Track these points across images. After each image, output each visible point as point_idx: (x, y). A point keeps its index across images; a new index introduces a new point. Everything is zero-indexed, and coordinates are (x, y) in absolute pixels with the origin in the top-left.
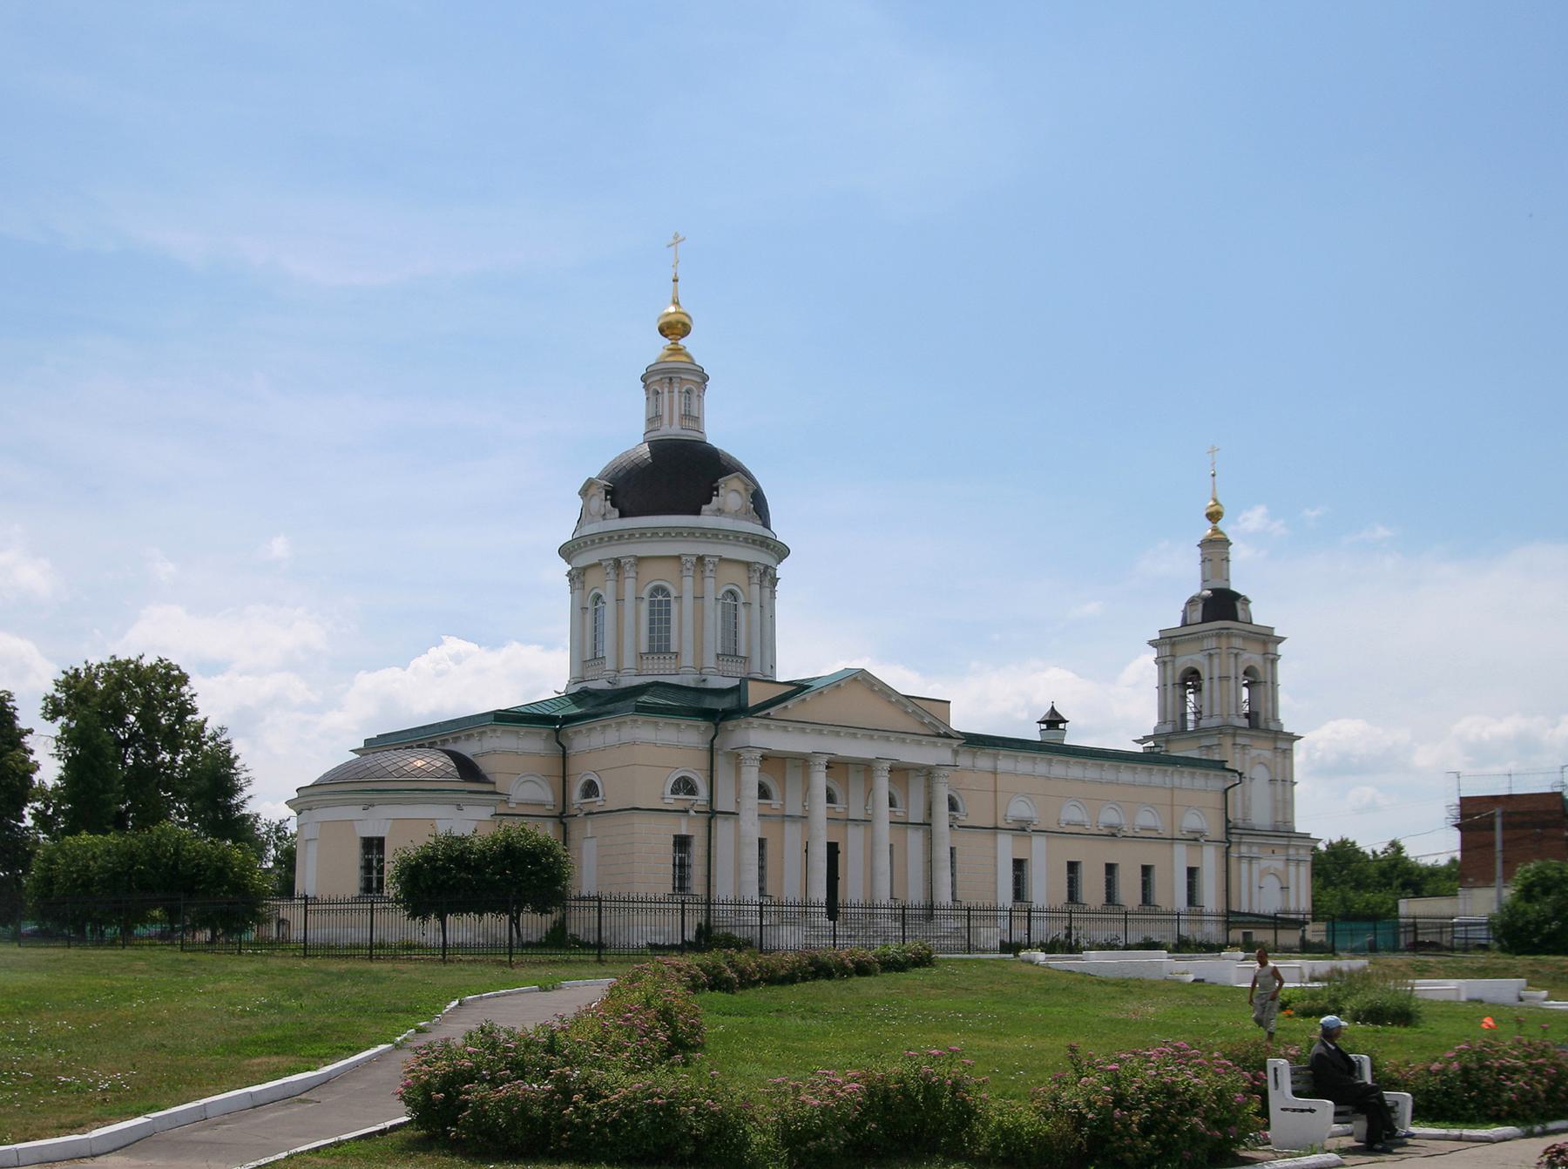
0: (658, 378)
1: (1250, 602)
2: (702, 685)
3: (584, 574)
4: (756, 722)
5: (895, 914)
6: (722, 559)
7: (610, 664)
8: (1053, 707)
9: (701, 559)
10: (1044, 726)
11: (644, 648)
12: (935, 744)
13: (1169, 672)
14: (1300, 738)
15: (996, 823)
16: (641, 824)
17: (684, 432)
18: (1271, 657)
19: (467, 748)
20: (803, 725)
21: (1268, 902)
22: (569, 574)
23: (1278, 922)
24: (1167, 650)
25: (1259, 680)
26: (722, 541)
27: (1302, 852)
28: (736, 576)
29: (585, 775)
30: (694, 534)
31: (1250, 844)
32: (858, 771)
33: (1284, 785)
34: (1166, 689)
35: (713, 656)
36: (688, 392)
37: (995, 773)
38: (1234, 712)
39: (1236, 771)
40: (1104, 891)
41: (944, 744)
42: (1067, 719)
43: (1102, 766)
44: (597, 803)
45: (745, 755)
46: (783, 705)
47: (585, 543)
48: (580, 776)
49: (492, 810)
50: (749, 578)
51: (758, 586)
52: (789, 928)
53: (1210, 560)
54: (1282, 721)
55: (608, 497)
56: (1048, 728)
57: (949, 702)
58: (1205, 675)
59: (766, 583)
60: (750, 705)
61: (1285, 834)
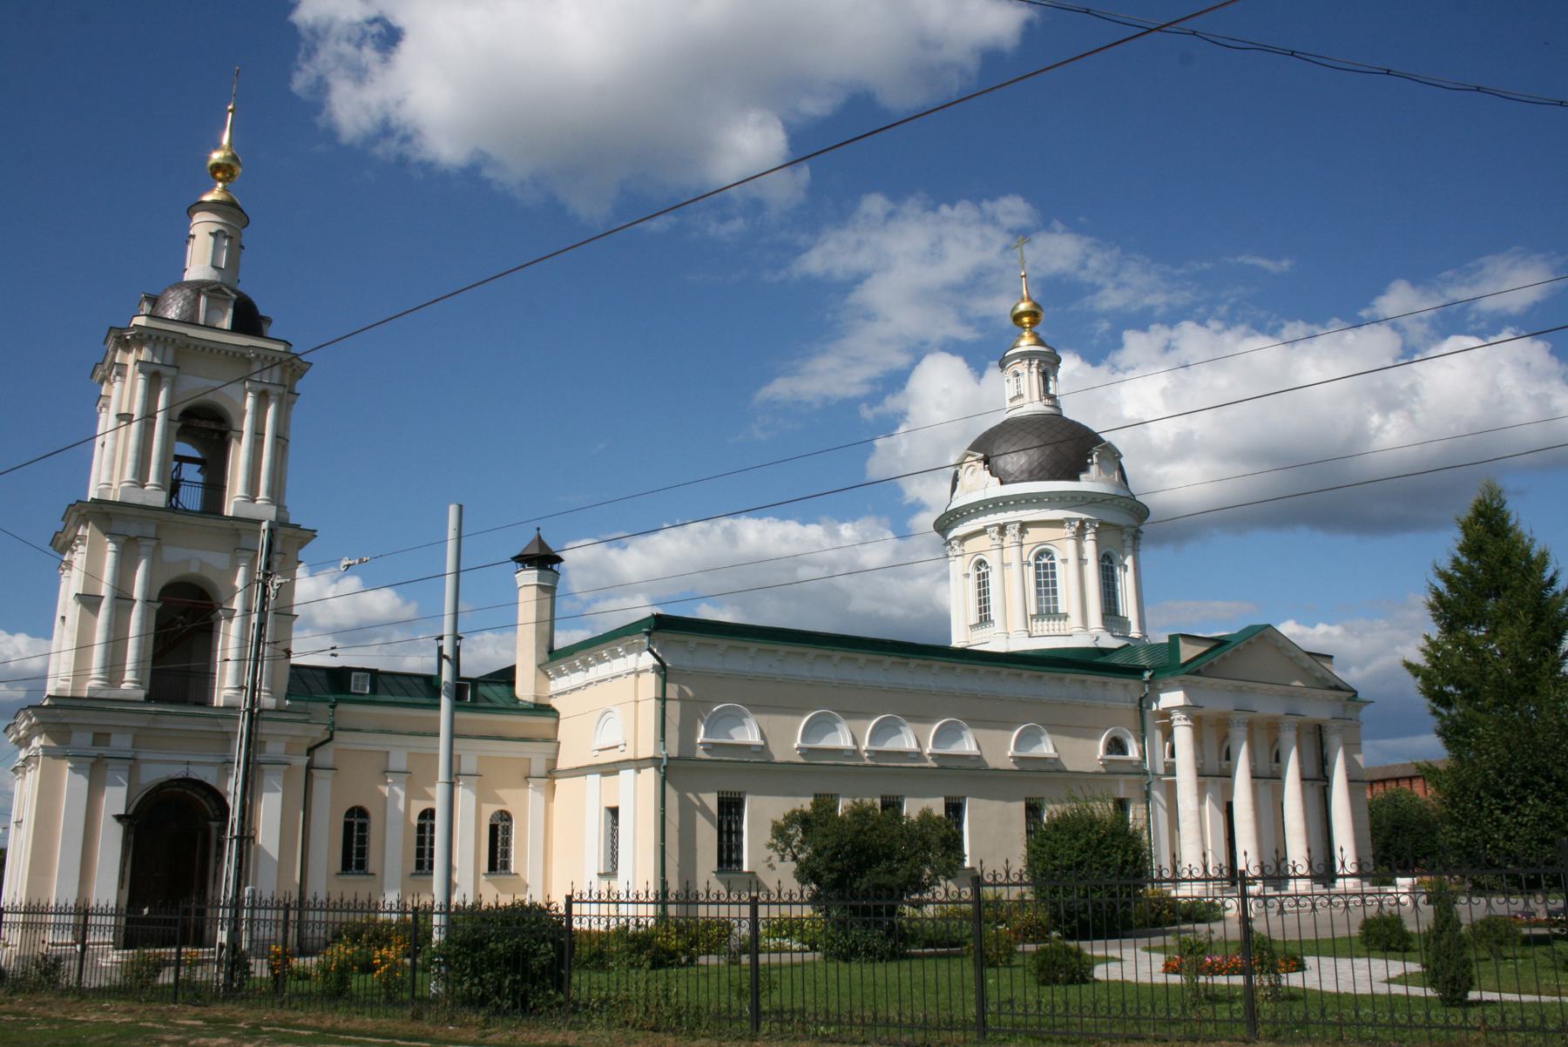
11: (1033, 610)
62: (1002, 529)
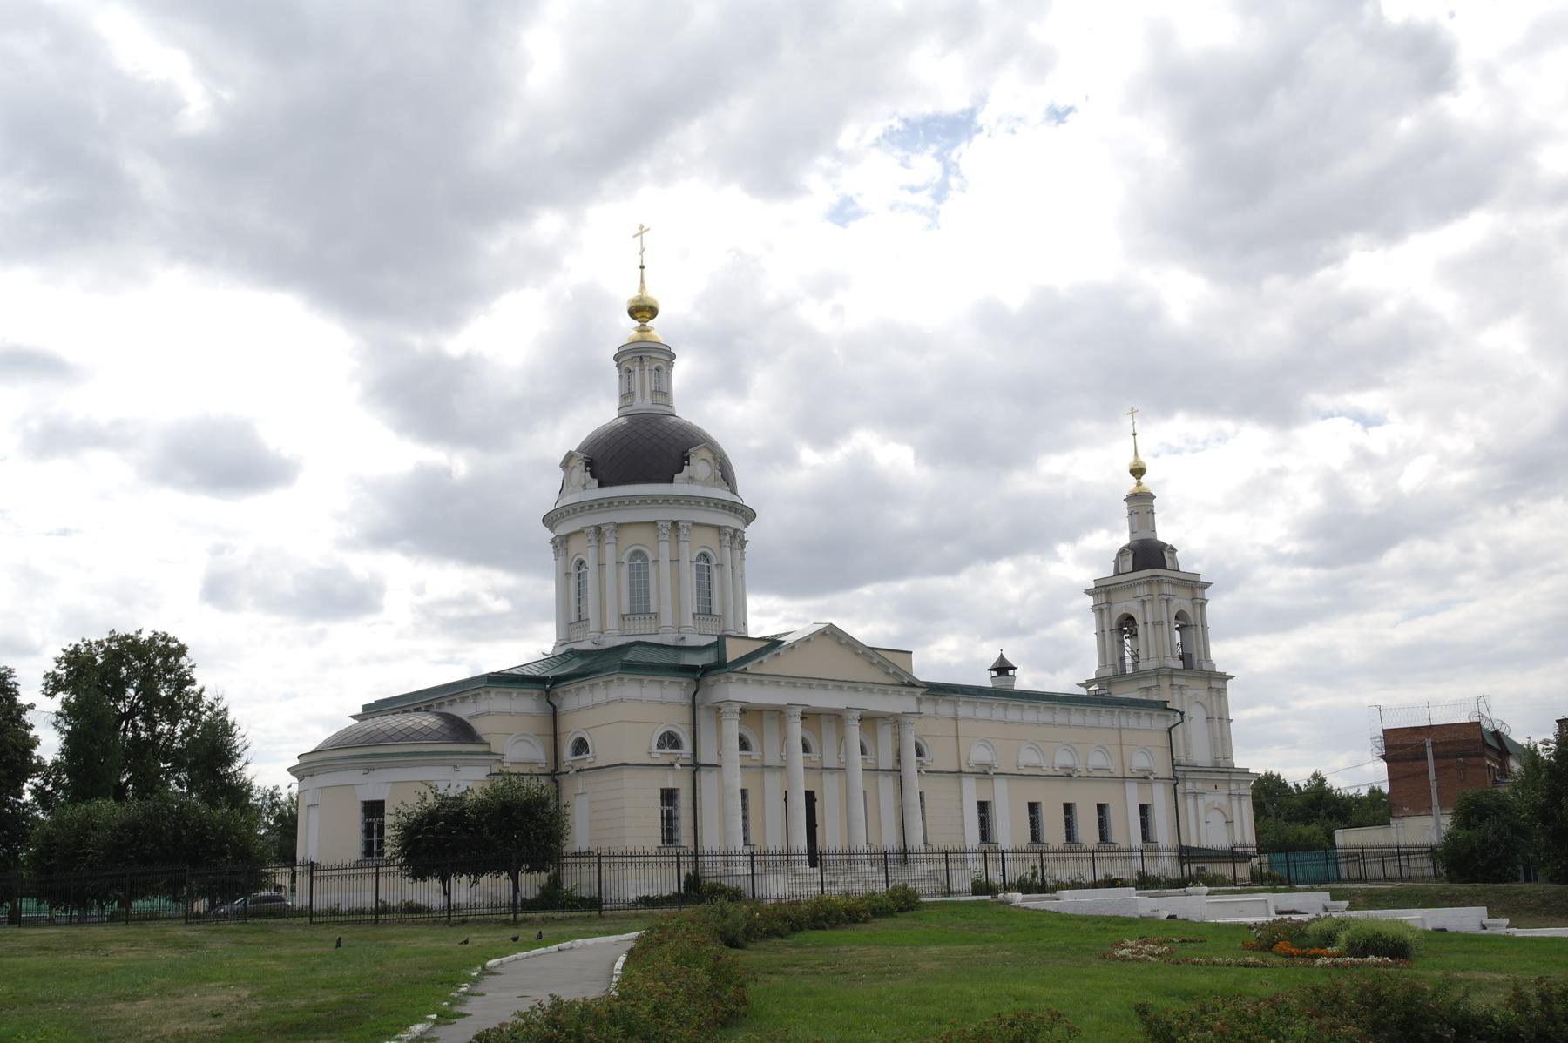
0: (629, 357)
1: (1176, 551)
2: (681, 644)
3: (567, 542)
4: (734, 677)
5: (871, 859)
6: (694, 524)
7: (593, 626)
8: (1001, 655)
9: (675, 524)
10: (995, 673)
11: (626, 610)
12: (899, 694)
13: (1106, 619)
14: (1232, 677)
15: (960, 767)
16: (629, 778)
17: (654, 407)
18: (1198, 601)
19: (463, 711)
20: (777, 679)
21: (1216, 838)
22: (553, 541)
23: (1232, 856)
24: (1103, 598)
25: (1190, 624)
26: (695, 507)
27: (1243, 786)
28: (708, 540)
29: (575, 733)
30: (668, 500)
31: (1194, 781)
32: (830, 721)
33: (1220, 723)
34: (1104, 635)
35: (691, 617)
36: (657, 369)
37: (956, 719)
38: (1169, 655)
39: (1178, 711)
40: (1065, 831)
41: (908, 693)
42: (1016, 666)
43: (1054, 709)
44: (586, 760)
45: (725, 709)
46: (759, 660)
47: (562, 513)
48: (570, 735)
49: (487, 770)
50: (720, 541)
51: (729, 549)
52: (775, 876)
53: (1137, 513)
54: (1214, 662)
55: (588, 468)
56: (1000, 674)
57: (911, 653)
58: (1139, 620)
59: (736, 545)
60: (728, 661)
61: (1226, 770)
62: (598, 530)
